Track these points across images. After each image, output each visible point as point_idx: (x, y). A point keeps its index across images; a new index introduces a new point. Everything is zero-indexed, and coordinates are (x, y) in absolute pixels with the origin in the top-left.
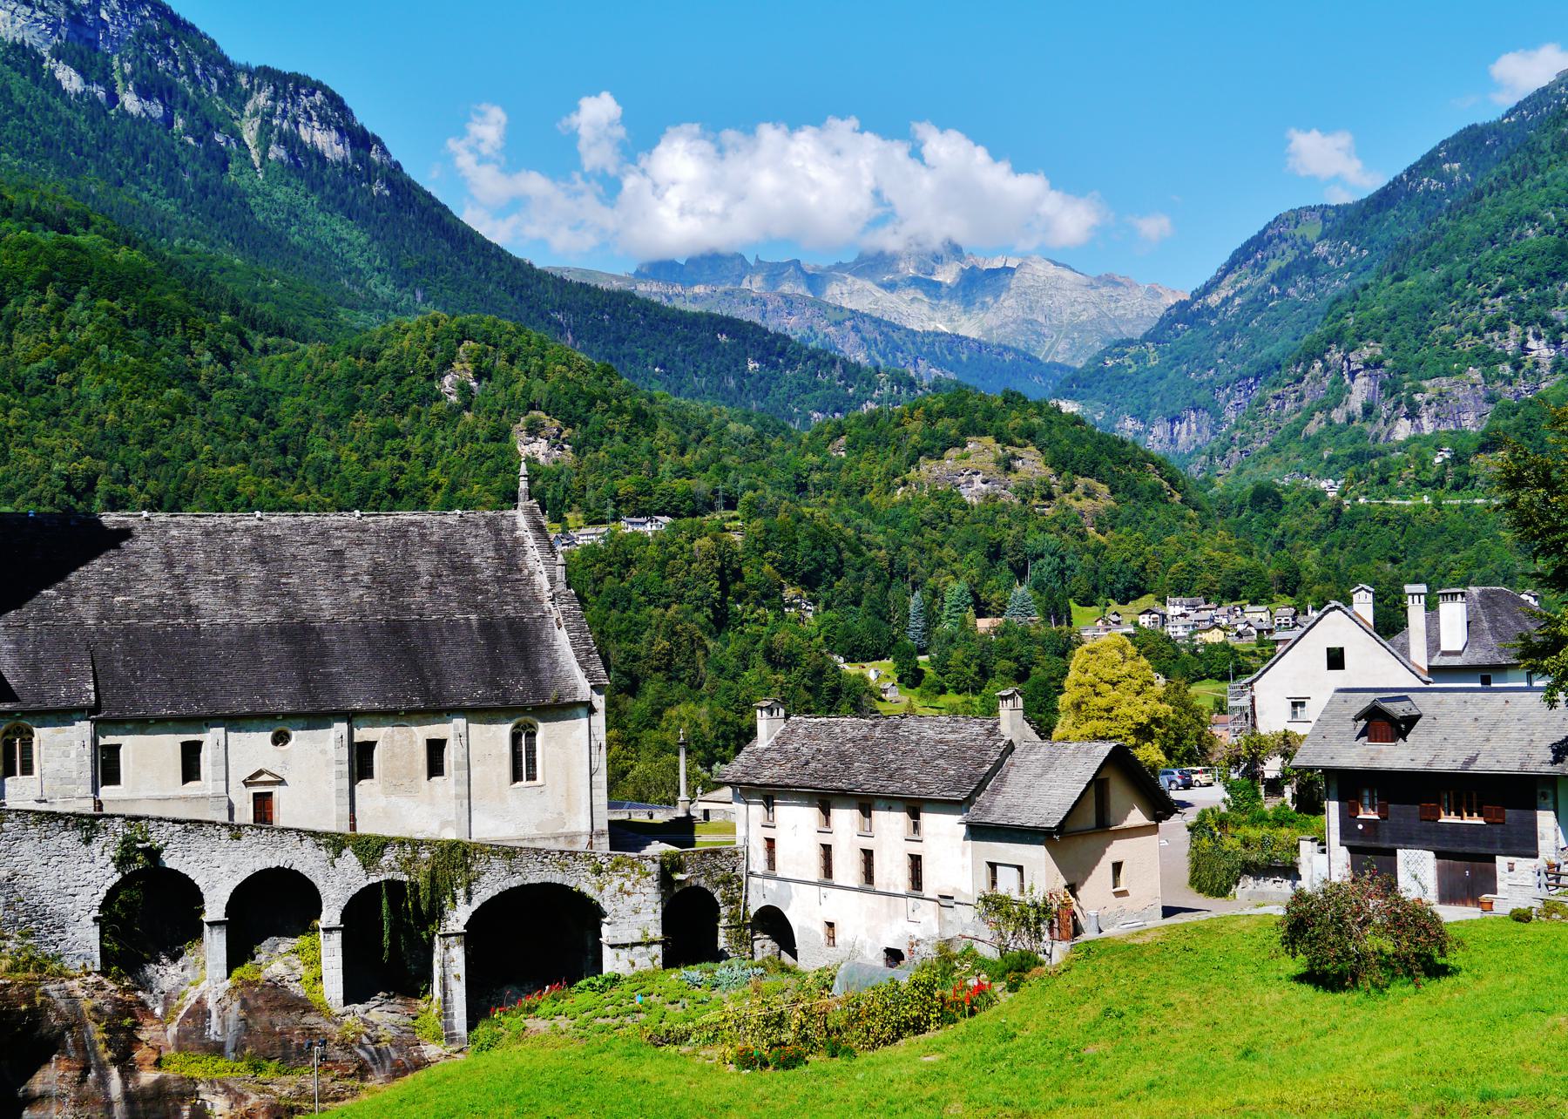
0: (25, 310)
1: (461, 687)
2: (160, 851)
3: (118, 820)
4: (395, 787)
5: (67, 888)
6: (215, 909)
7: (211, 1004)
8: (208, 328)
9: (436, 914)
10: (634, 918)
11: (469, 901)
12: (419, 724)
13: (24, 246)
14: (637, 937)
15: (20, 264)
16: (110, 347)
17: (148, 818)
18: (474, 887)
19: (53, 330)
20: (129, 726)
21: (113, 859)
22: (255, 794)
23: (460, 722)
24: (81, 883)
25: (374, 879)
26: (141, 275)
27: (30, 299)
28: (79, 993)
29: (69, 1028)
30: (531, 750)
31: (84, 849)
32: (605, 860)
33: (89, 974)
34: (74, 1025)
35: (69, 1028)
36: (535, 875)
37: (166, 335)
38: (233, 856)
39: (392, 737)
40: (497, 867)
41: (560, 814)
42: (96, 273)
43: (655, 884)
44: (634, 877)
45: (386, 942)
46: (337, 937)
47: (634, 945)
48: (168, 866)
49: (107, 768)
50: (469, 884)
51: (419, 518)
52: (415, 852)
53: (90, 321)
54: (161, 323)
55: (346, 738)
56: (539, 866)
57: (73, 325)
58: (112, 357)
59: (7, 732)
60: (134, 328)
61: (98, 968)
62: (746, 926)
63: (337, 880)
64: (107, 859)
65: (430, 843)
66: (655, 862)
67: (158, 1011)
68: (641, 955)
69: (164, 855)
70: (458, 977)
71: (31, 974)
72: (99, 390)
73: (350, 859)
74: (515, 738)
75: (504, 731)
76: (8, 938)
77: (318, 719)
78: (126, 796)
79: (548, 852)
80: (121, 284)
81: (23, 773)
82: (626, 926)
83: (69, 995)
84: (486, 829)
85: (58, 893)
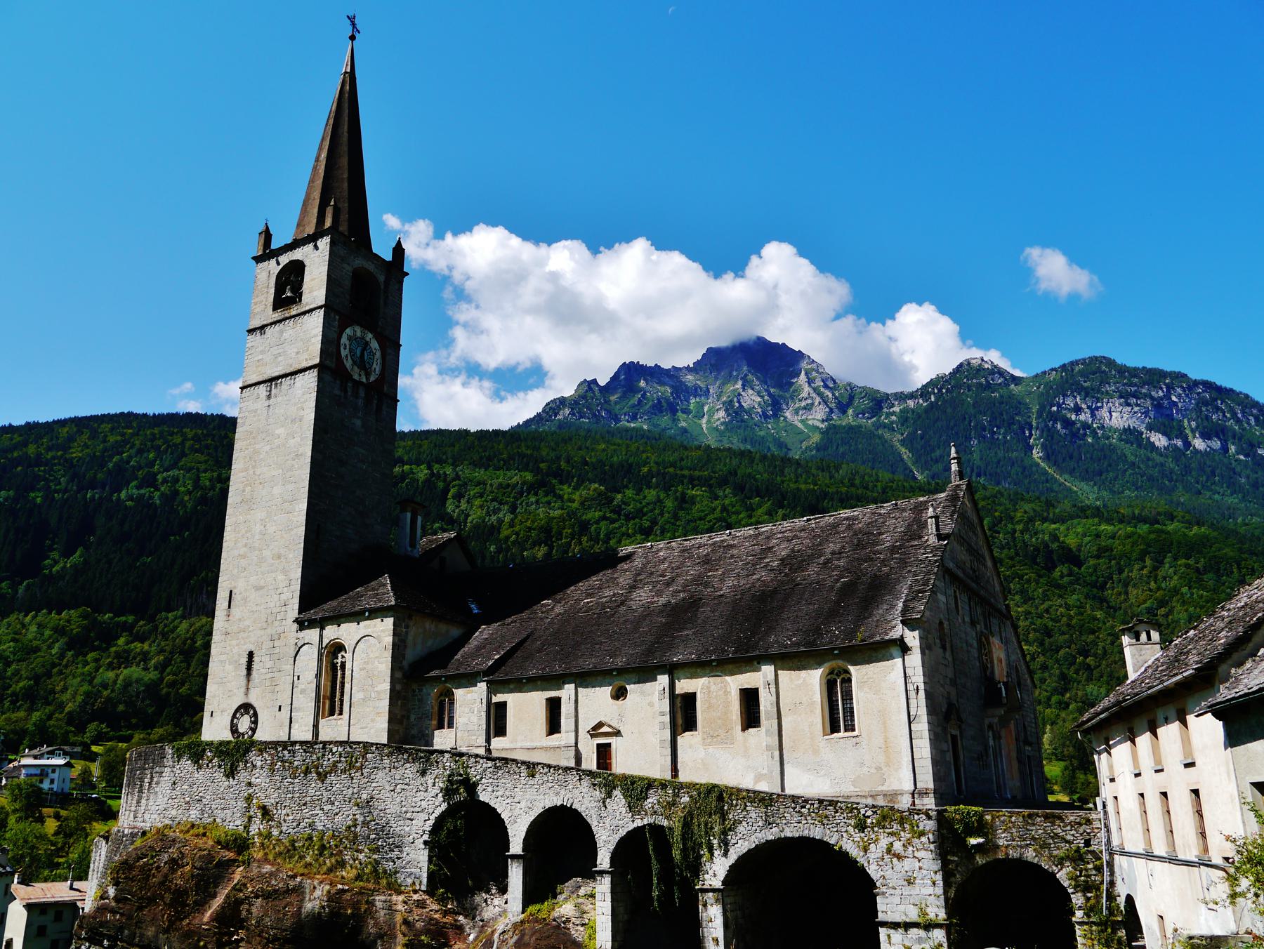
0: (1135, 574)
1: (785, 637)
2: (475, 785)
3: (447, 755)
4: (713, 738)
5: (406, 812)
6: (516, 847)
7: (496, 937)
8: (1256, 566)
9: (696, 869)
10: (907, 890)
11: (726, 854)
12: (732, 674)
13: (1129, 536)
14: (913, 916)
15: (1128, 547)
16: (1190, 588)
17: (470, 756)
18: (732, 838)
19: (1152, 583)
20: (512, 686)
21: (441, 789)
22: (598, 745)
23: (768, 670)
24: (417, 809)
25: (639, 823)
26: (1205, 540)
27: (1136, 567)
28: (400, 907)
29: (381, 936)
30: (848, 696)
31: (421, 780)
32: (870, 813)
33: (415, 892)
34: (385, 934)
35: (381, 936)
36: (792, 828)
37: (1227, 575)
38: (531, 793)
39: (708, 688)
40: (753, 815)
41: (879, 768)
42: (1174, 546)
43: (932, 847)
44: (906, 835)
45: (655, 893)
46: (607, 880)
47: (907, 926)
48: (481, 799)
49: (497, 721)
50: (724, 833)
51: (856, 513)
52: (676, 795)
53: (1175, 574)
54: (1222, 568)
55: (667, 690)
56: (796, 817)
57: (1164, 578)
58: (1192, 594)
59: (441, 695)
60: (1204, 574)
61: (424, 888)
62: (1116, 926)
63: (607, 821)
64: (436, 790)
65: (692, 786)
66: (929, 817)
67: (471, 937)
68: (920, 940)
69: (480, 788)
70: (716, 941)
71: (371, 886)
72: (1184, 616)
73: (618, 801)
74: (830, 686)
75: (814, 678)
76: (361, 851)
77: (645, 674)
78: (508, 746)
79: (806, 801)
80: (1191, 548)
81: (449, 727)
82: (897, 900)
83: (391, 909)
84: (800, 783)
85: (400, 816)
